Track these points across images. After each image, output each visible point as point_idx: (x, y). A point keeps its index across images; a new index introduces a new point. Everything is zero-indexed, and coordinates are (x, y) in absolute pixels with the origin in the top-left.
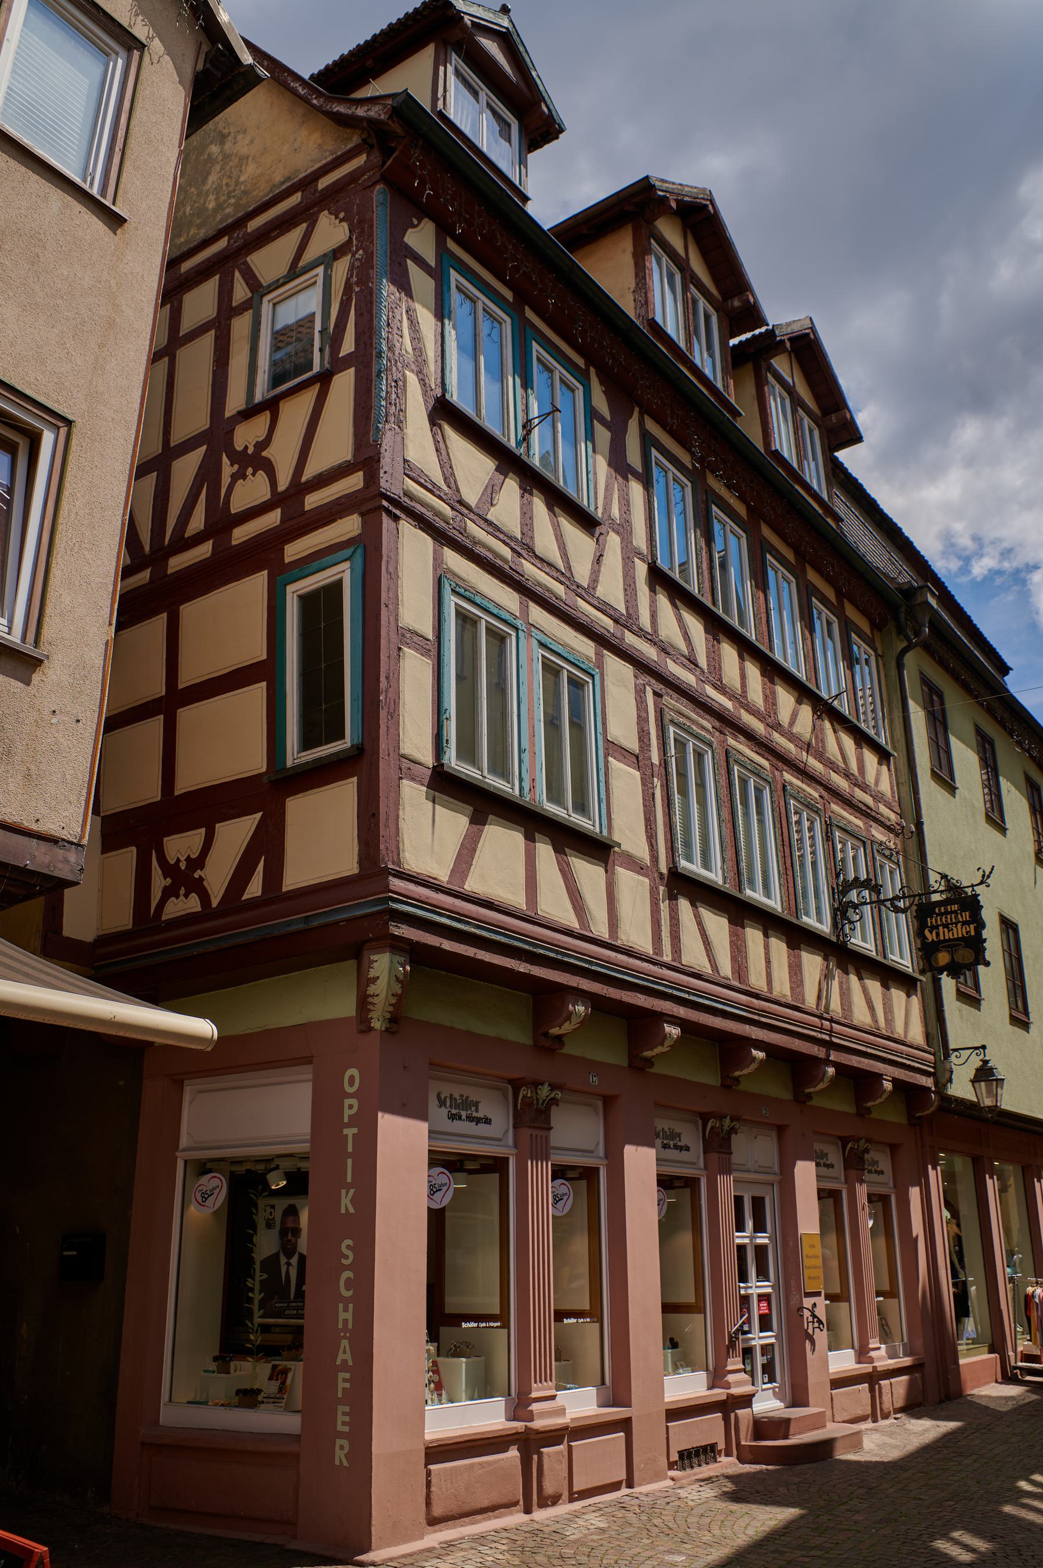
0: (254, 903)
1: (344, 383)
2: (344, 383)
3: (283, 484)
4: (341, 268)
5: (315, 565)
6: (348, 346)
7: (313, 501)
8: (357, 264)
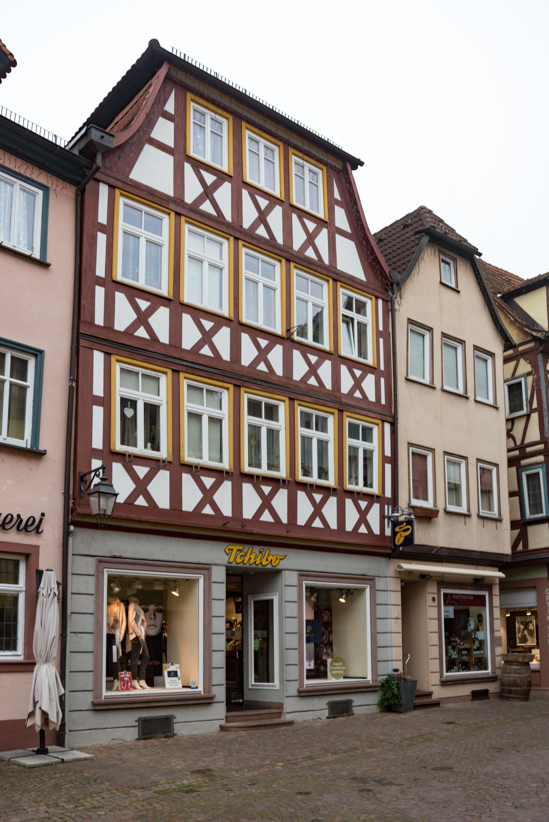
0: (520, 552)
1: (535, 417)
2: (535, 417)
3: (519, 442)
4: (530, 379)
5: (531, 467)
6: (535, 405)
7: (529, 450)
8: (535, 379)
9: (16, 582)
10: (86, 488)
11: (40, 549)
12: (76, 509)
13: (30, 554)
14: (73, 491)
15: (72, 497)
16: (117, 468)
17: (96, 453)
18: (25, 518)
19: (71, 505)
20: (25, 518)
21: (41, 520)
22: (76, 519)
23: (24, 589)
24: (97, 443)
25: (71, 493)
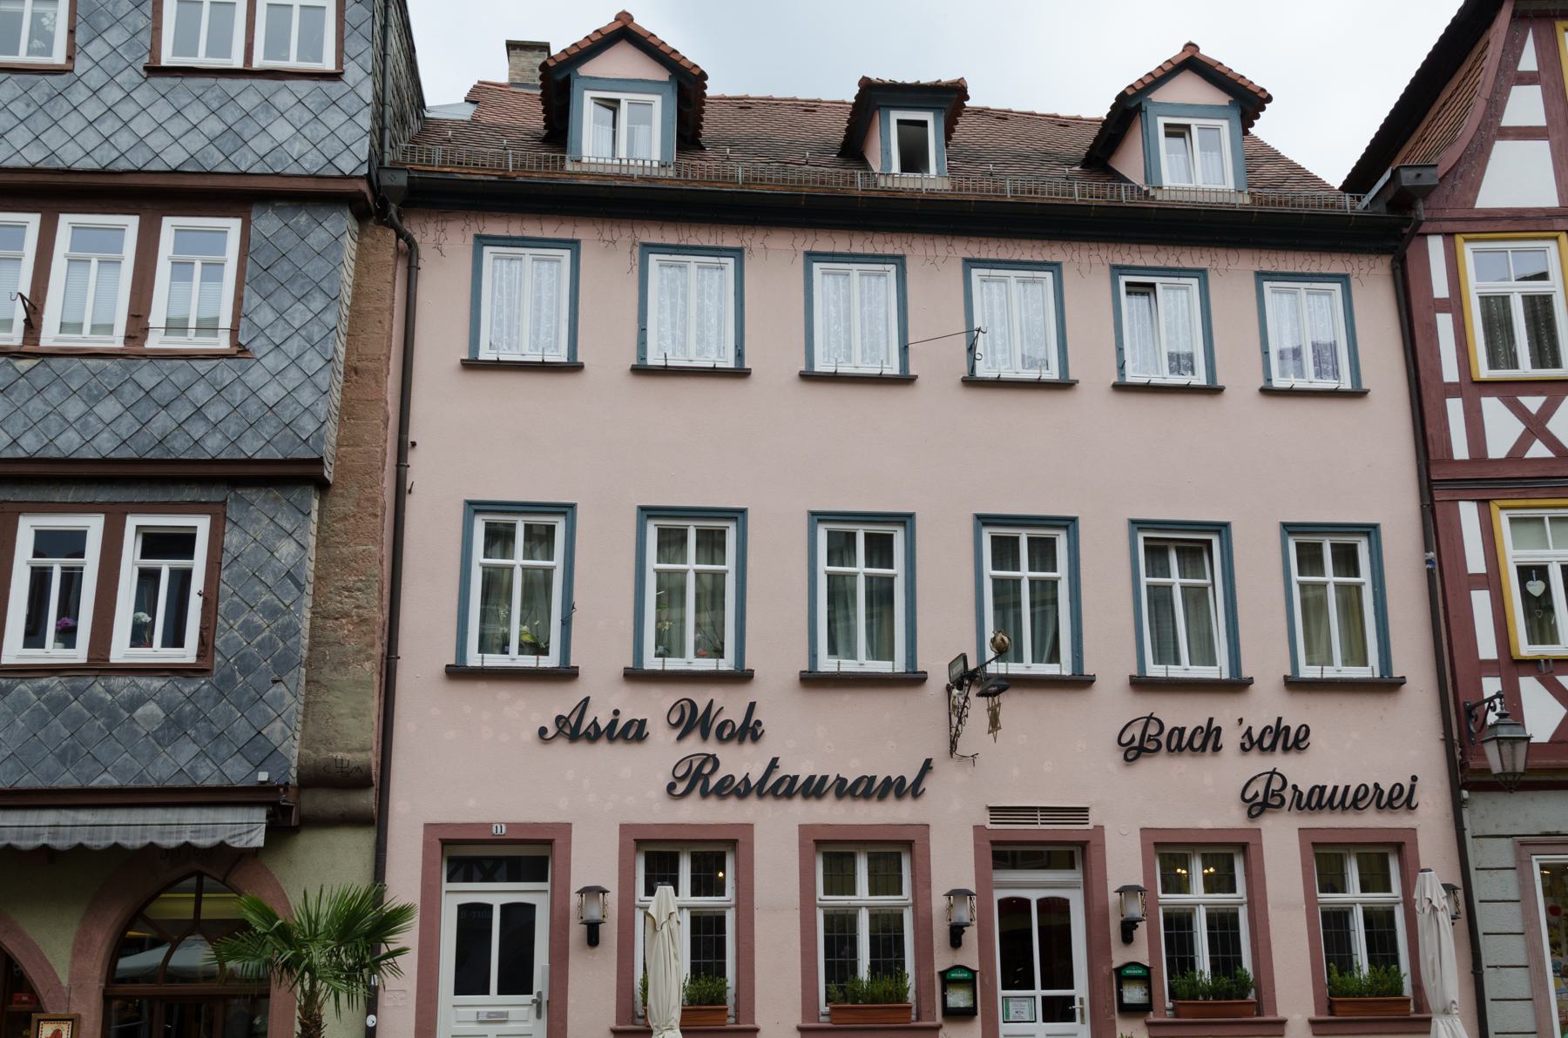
9: (1387, 889)
10: (1479, 728)
11: (1419, 833)
12: (1468, 763)
13: (1403, 843)
14: (1459, 734)
15: (1458, 744)
16: (1529, 687)
17: (1489, 667)
18: (1386, 788)
19: (1459, 757)
20: (1386, 788)
21: (1412, 788)
22: (1469, 779)
23: (1401, 898)
24: (1487, 648)
25: (1456, 737)
